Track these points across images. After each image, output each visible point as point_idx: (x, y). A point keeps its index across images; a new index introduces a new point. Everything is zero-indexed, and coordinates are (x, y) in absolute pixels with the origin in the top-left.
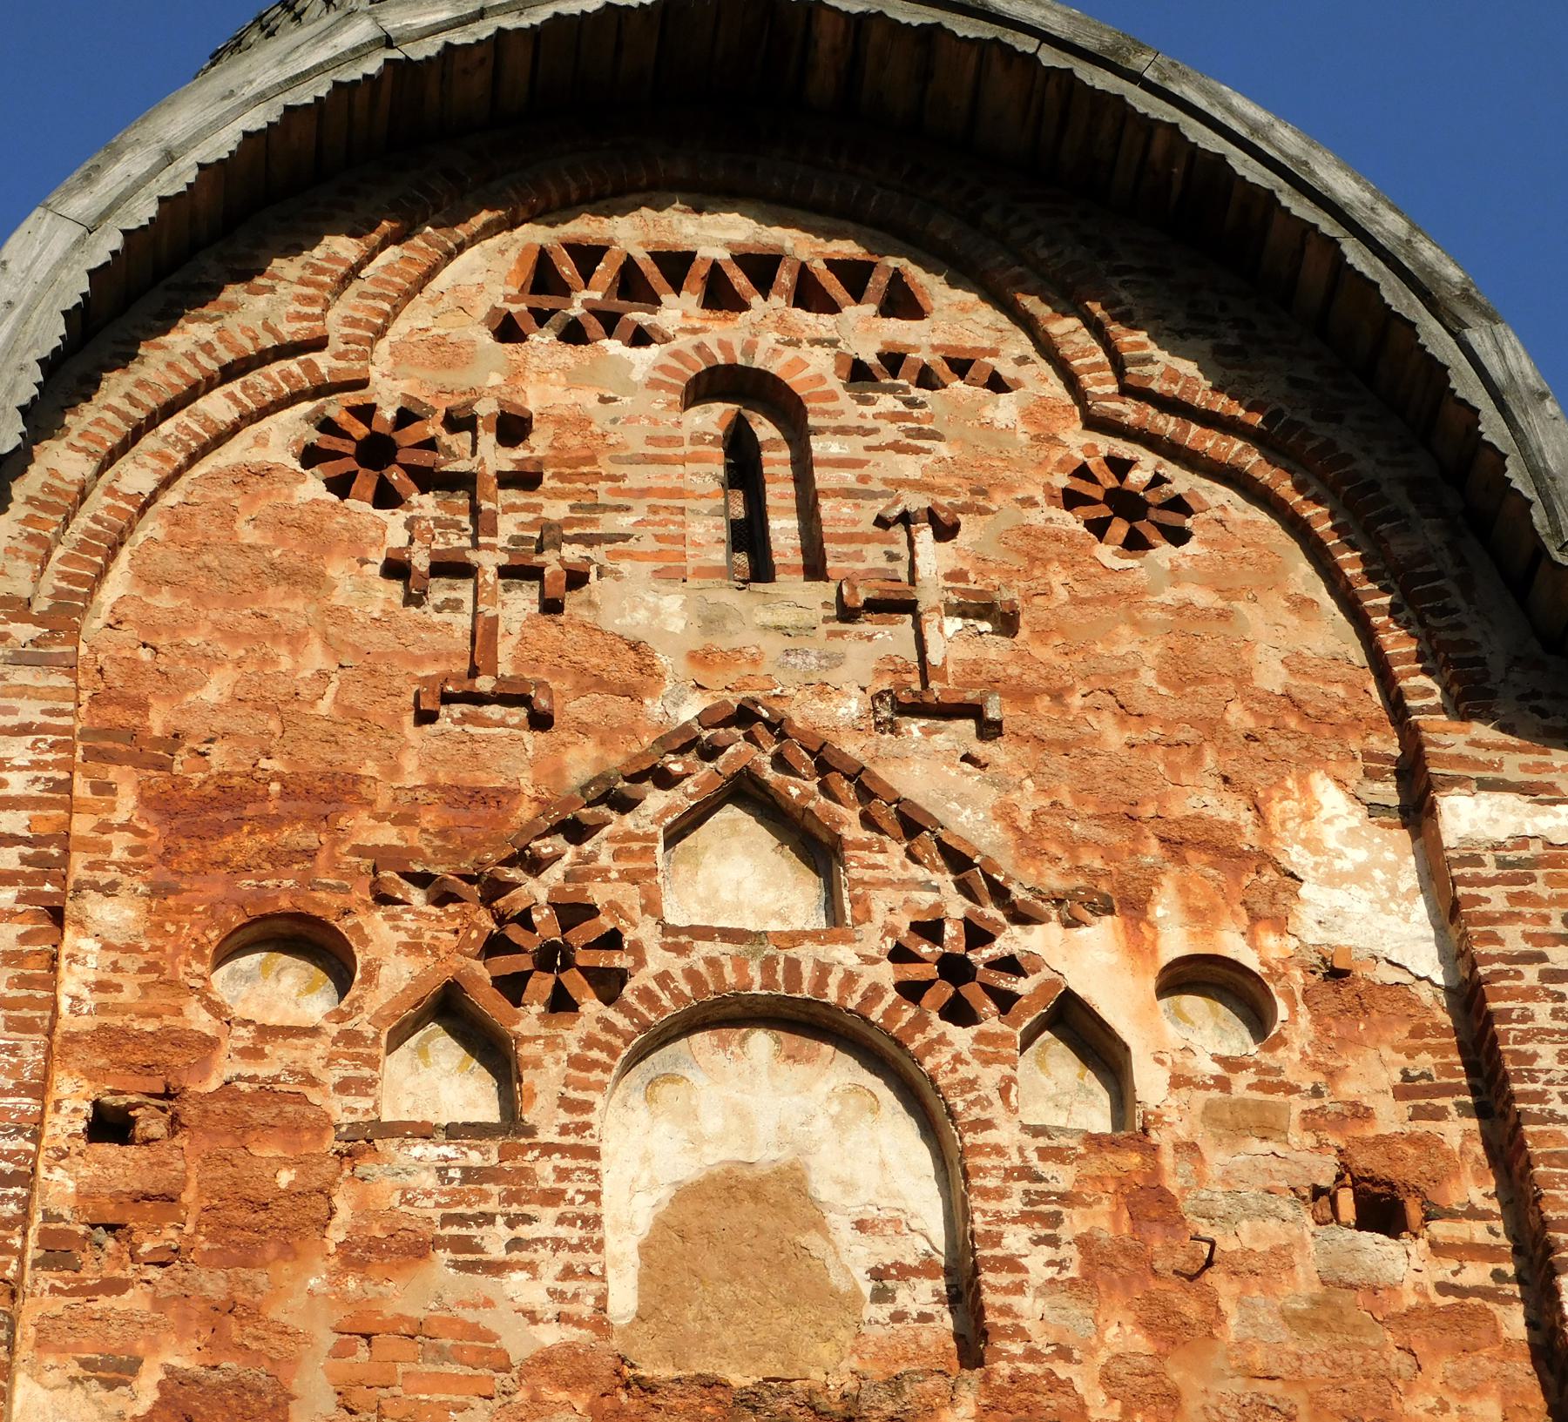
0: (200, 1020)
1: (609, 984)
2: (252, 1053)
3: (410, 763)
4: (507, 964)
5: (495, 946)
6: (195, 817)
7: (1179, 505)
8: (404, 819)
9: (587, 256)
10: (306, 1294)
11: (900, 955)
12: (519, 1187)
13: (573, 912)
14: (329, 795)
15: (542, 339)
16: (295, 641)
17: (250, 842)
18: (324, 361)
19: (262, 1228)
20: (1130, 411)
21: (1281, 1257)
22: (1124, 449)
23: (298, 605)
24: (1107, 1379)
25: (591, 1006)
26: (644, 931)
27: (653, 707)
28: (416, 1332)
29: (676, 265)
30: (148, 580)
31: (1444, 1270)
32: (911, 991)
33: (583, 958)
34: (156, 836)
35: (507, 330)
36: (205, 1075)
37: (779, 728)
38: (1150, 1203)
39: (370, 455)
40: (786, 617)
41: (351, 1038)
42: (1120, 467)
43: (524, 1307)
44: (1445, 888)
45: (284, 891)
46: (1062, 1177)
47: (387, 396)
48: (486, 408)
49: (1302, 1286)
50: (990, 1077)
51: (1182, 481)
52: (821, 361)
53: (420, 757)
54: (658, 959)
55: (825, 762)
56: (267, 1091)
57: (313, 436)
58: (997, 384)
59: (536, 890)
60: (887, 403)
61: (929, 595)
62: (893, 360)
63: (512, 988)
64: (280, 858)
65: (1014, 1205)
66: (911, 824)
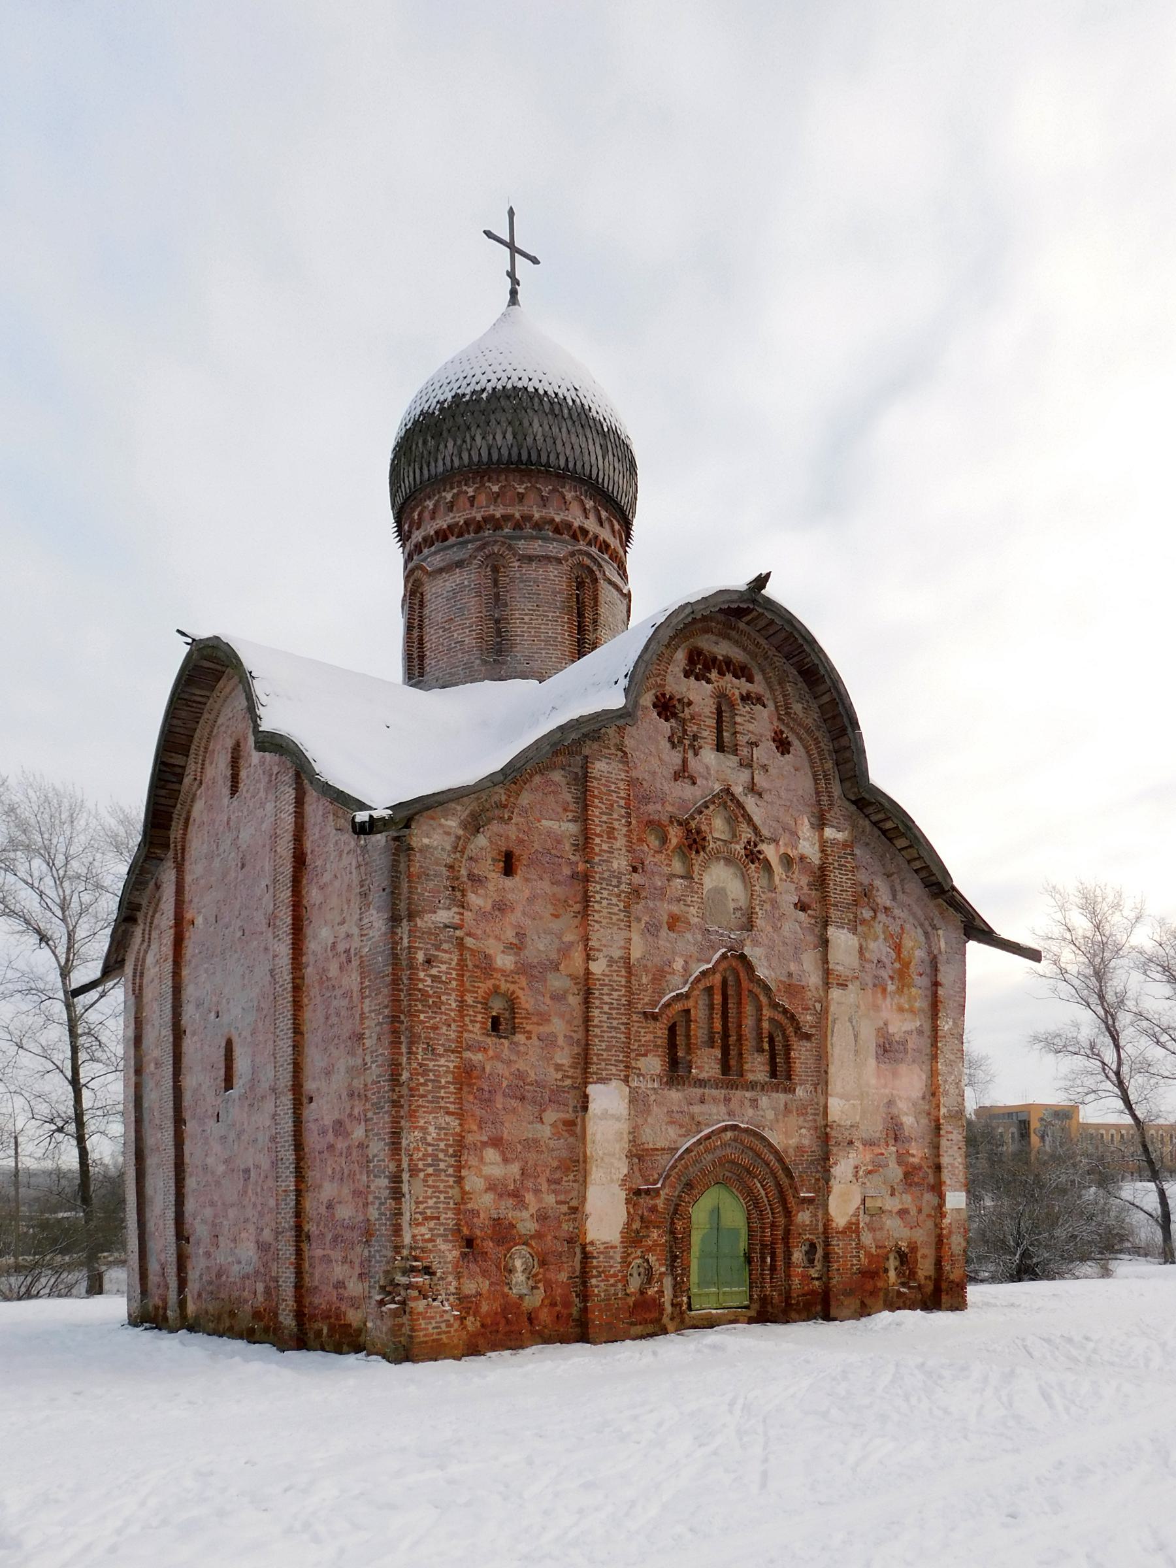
44: (824, 845)
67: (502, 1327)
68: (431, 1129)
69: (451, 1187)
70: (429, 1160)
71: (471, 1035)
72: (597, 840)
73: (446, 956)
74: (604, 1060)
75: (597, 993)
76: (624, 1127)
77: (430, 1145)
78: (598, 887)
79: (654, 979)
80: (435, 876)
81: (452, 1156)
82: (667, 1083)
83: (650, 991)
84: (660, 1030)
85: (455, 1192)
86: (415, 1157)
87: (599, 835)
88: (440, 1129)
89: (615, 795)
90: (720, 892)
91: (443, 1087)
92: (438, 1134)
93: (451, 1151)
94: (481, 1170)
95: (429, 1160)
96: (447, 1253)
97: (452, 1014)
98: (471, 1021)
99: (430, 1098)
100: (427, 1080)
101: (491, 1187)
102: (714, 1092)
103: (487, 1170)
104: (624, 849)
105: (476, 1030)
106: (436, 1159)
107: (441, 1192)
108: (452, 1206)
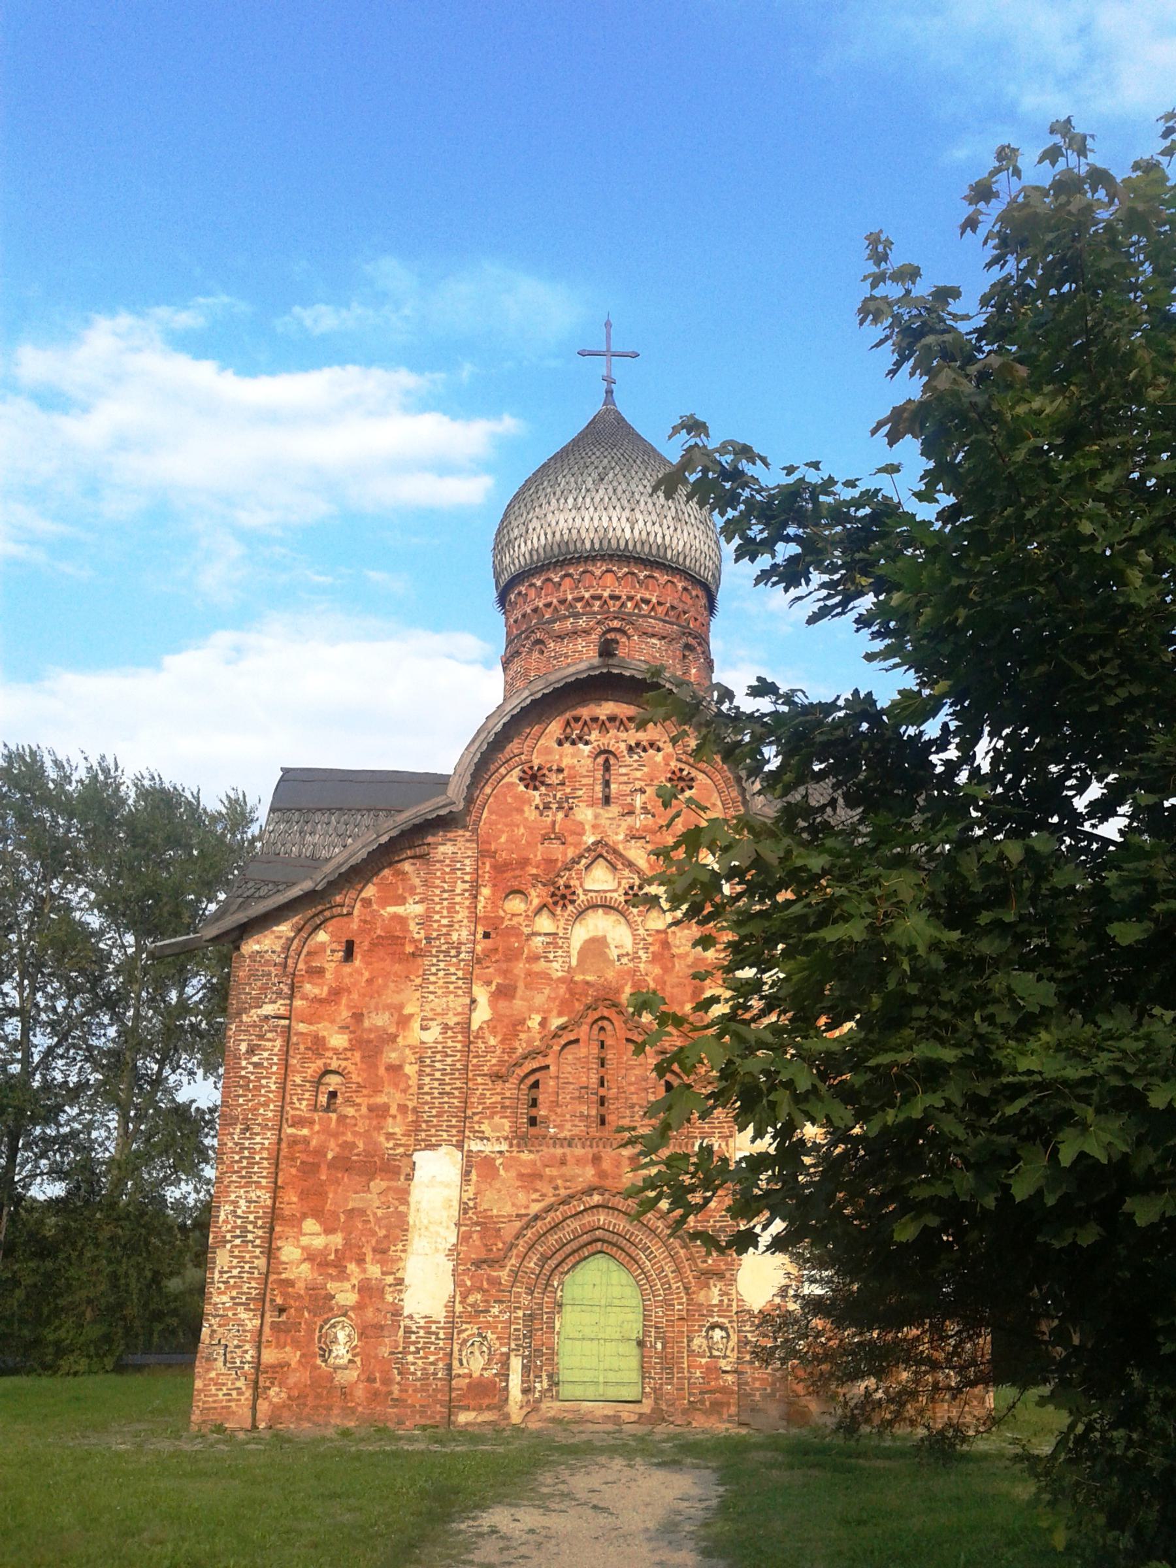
0: (502, 913)
1: (573, 902)
2: (511, 920)
3: (539, 854)
4: (555, 898)
5: (553, 895)
6: (500, 869)
7: (692, 779)
8: (537, 867)
9: (577, 719)
10: (520, 967)
11: (626, 894)
12: (556, 946)
13: (567, 887)
14: (524, 862)
15: (567, 745)
16: (518, 826)
17: (509, 875)
18: (523, 757)
19: (512, 955)
20: (684, 757)
21: (687, 954)
22: (683, 766)
23: (518, 817)
24: (654, 980)
25: (570, 908)
26: (580, 891)
27: (585, 838)
28: (537, 974)
29: (595, 720)
30: (491, 812)
31: (717, 955)
32: (626, 902)
33: (569, 897)
34: (493, 874)
35: (560, 743)
36: (502, 923)
37: (606, 845)
38: (666, 944)
39: (533, 778)
40: (610, 816)
41: (527, 916)
42: (681, 770)
43: (556, 969)
45: (515, 884)
46: (650, 940)
47: (536, 763)
48: (555, 768)
49: (690, 960)
50: (639, 919)
51: (694, 773)
52: (623, 746)
53: (539, 853)
54: (582, 897)
55: (615, 852)
56: (513, 927)
57: (521, 774)
58: (659, 750)
59: (561, 882)
60: (636, 757)
61: (638, 811)
62: (638, 744)
63: (556, 903)
64: (515, 877)
65: (641, 946)
66: (630, 865)
67: (310, 1401)
68: (242, 1203)
69: (257, 1258)
70: (238, 1232)
71: (298, 1113)
72: (437, 917)
73: (269, 1044)
74: (434, 1126)
75: (428, 1061)
76: (455, 1194)
77: (239, 1217)
78: (435, 960)
79: (502, 1042)
80: (263, 976)
81: (261, 1227)
82: (519, 1145)
83: (499, 1052)
84: (509, 1089)
85: (261, 1262)
86: (224, 1229)
87: (438, 912)
88: (250, 1202)
89: (459, 873)
90: (596, 945)
91: (258, 1163)
92: (248, 1207)
93: (260, 1223)
94: (298, 1241)
95: (238, 1232)
96: (247, 1322)
97: (271, 1095)
98: (299, 1099)
99: (244, 1173)
100: (242, 1158)
101: (310, 1256)
102: (579, 1151)
103: (304, 1241)
104: (465, 921)
105: (302, 1107)
106: (245, 1231)
107: (246, 1262)
108: (256, 1275)
